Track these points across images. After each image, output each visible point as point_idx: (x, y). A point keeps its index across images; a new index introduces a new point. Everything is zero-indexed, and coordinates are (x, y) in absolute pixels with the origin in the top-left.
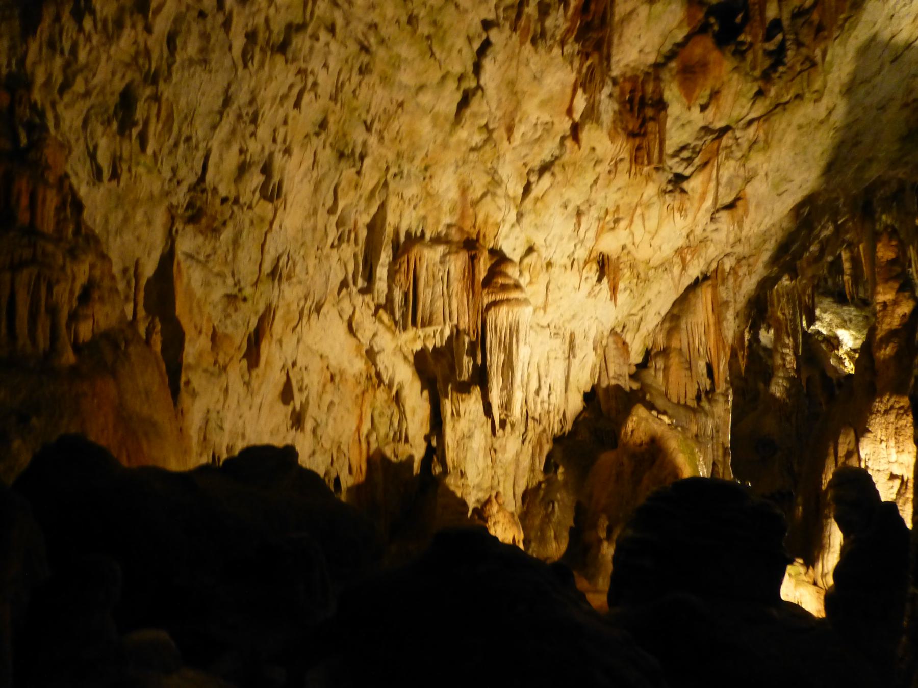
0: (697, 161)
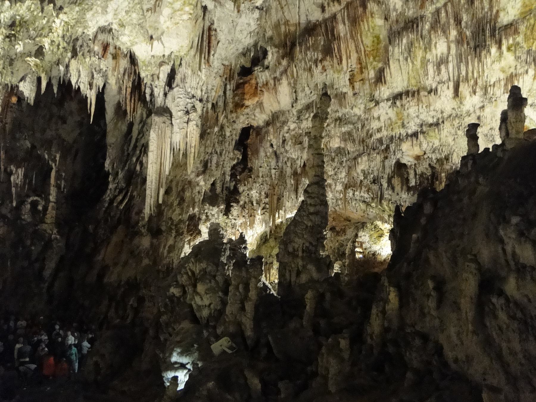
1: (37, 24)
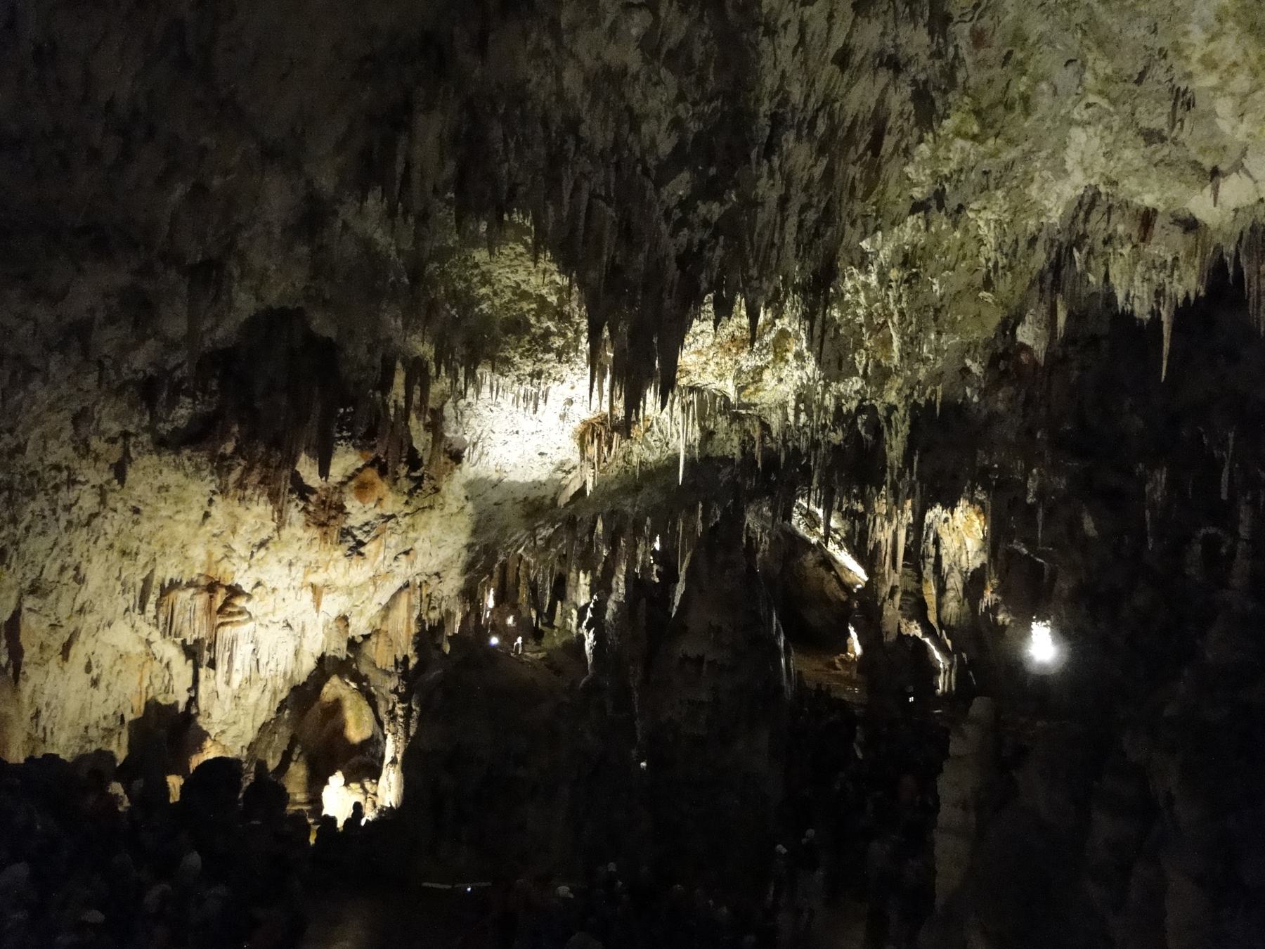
0: (373, 534)
1: (945, 243)
